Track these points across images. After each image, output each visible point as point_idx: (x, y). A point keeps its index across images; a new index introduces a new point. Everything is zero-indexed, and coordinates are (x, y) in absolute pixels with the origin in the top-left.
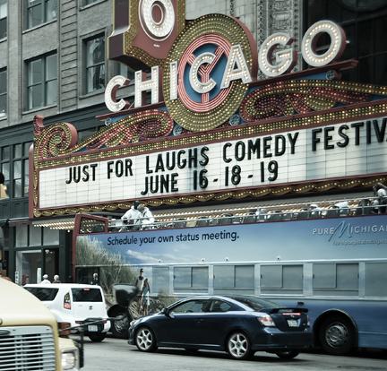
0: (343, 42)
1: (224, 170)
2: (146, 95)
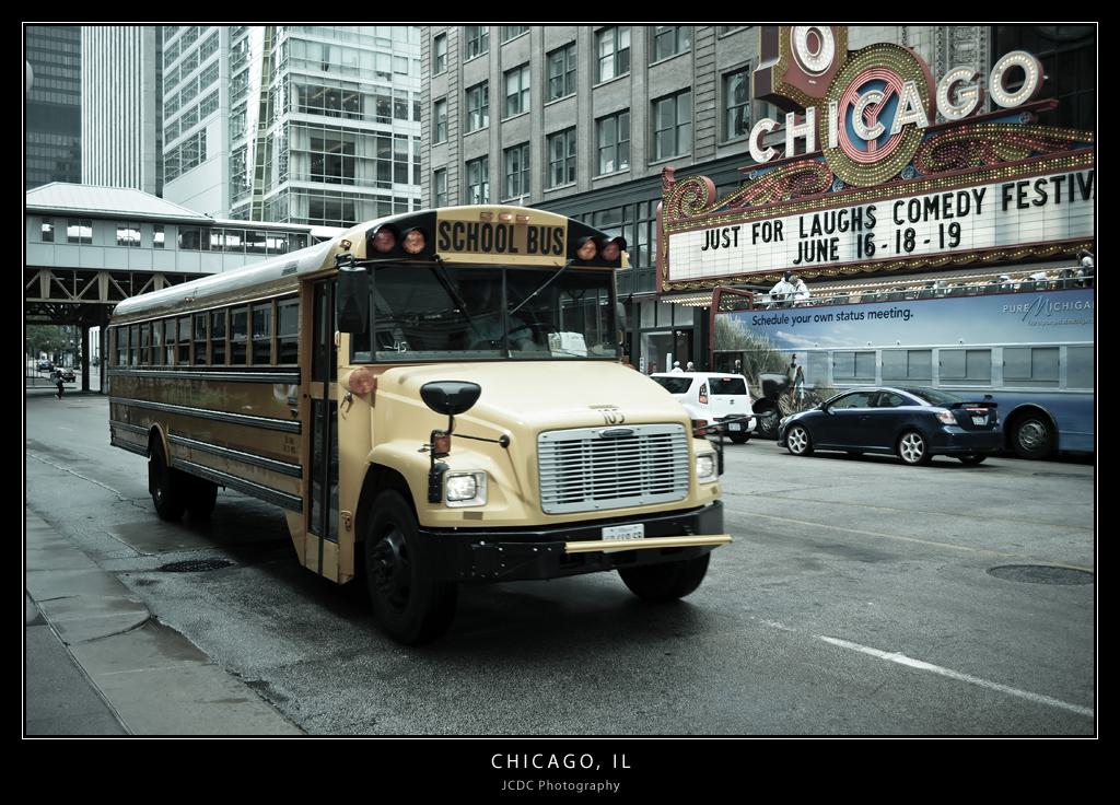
0: (1040, 78)
1: (895, 234)
2: (800, 142)
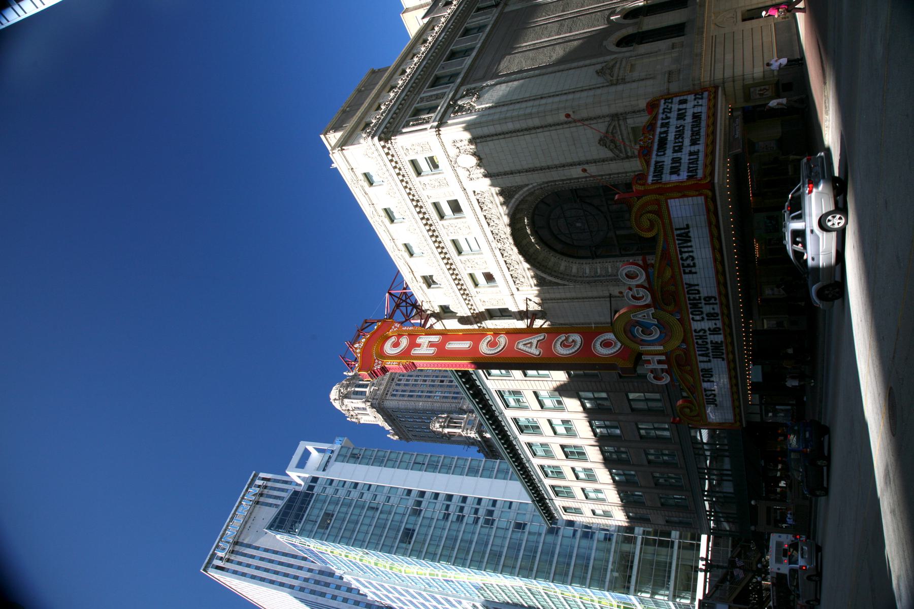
2: (659, 362)
